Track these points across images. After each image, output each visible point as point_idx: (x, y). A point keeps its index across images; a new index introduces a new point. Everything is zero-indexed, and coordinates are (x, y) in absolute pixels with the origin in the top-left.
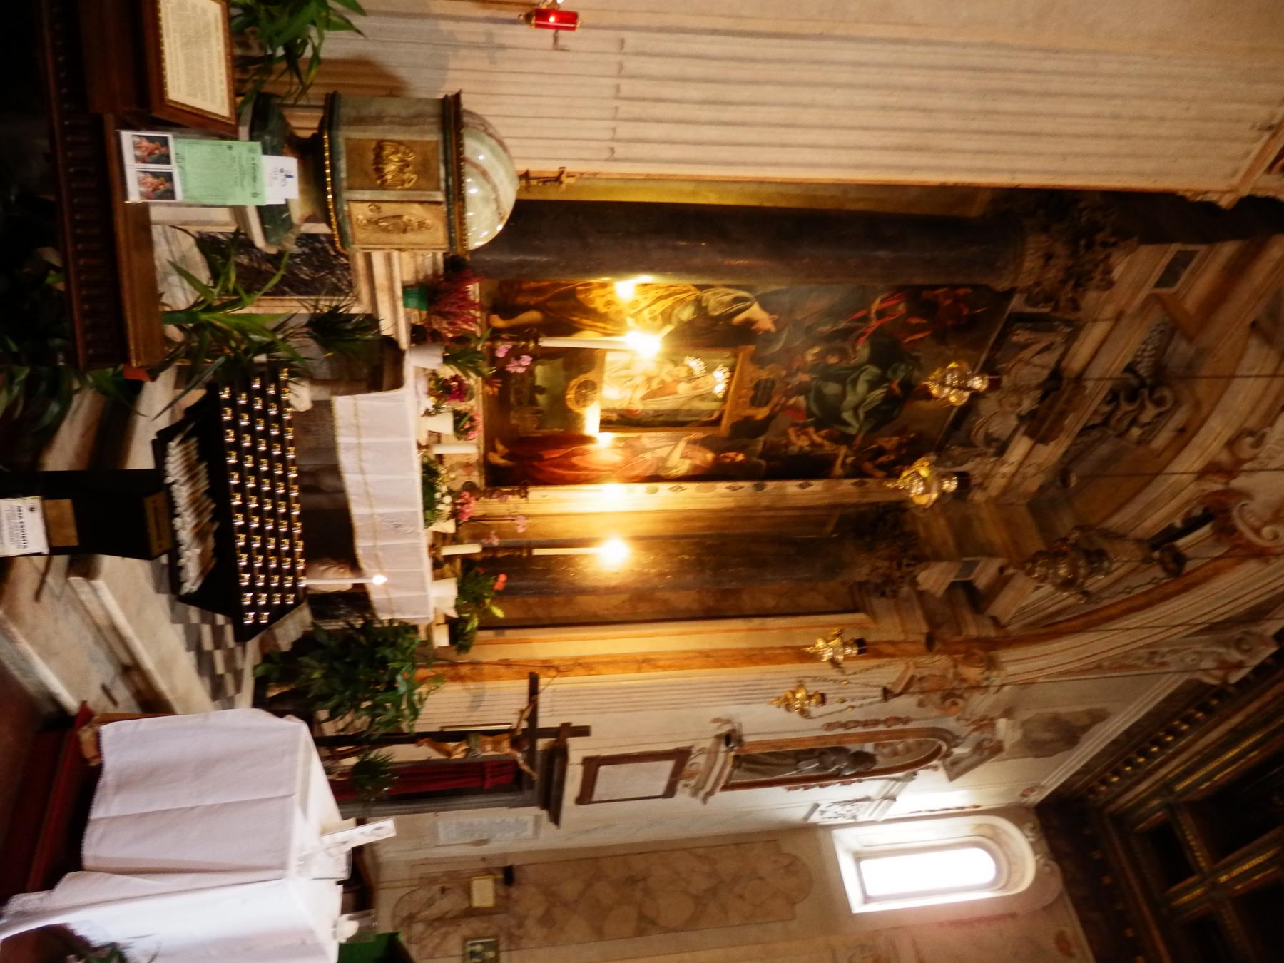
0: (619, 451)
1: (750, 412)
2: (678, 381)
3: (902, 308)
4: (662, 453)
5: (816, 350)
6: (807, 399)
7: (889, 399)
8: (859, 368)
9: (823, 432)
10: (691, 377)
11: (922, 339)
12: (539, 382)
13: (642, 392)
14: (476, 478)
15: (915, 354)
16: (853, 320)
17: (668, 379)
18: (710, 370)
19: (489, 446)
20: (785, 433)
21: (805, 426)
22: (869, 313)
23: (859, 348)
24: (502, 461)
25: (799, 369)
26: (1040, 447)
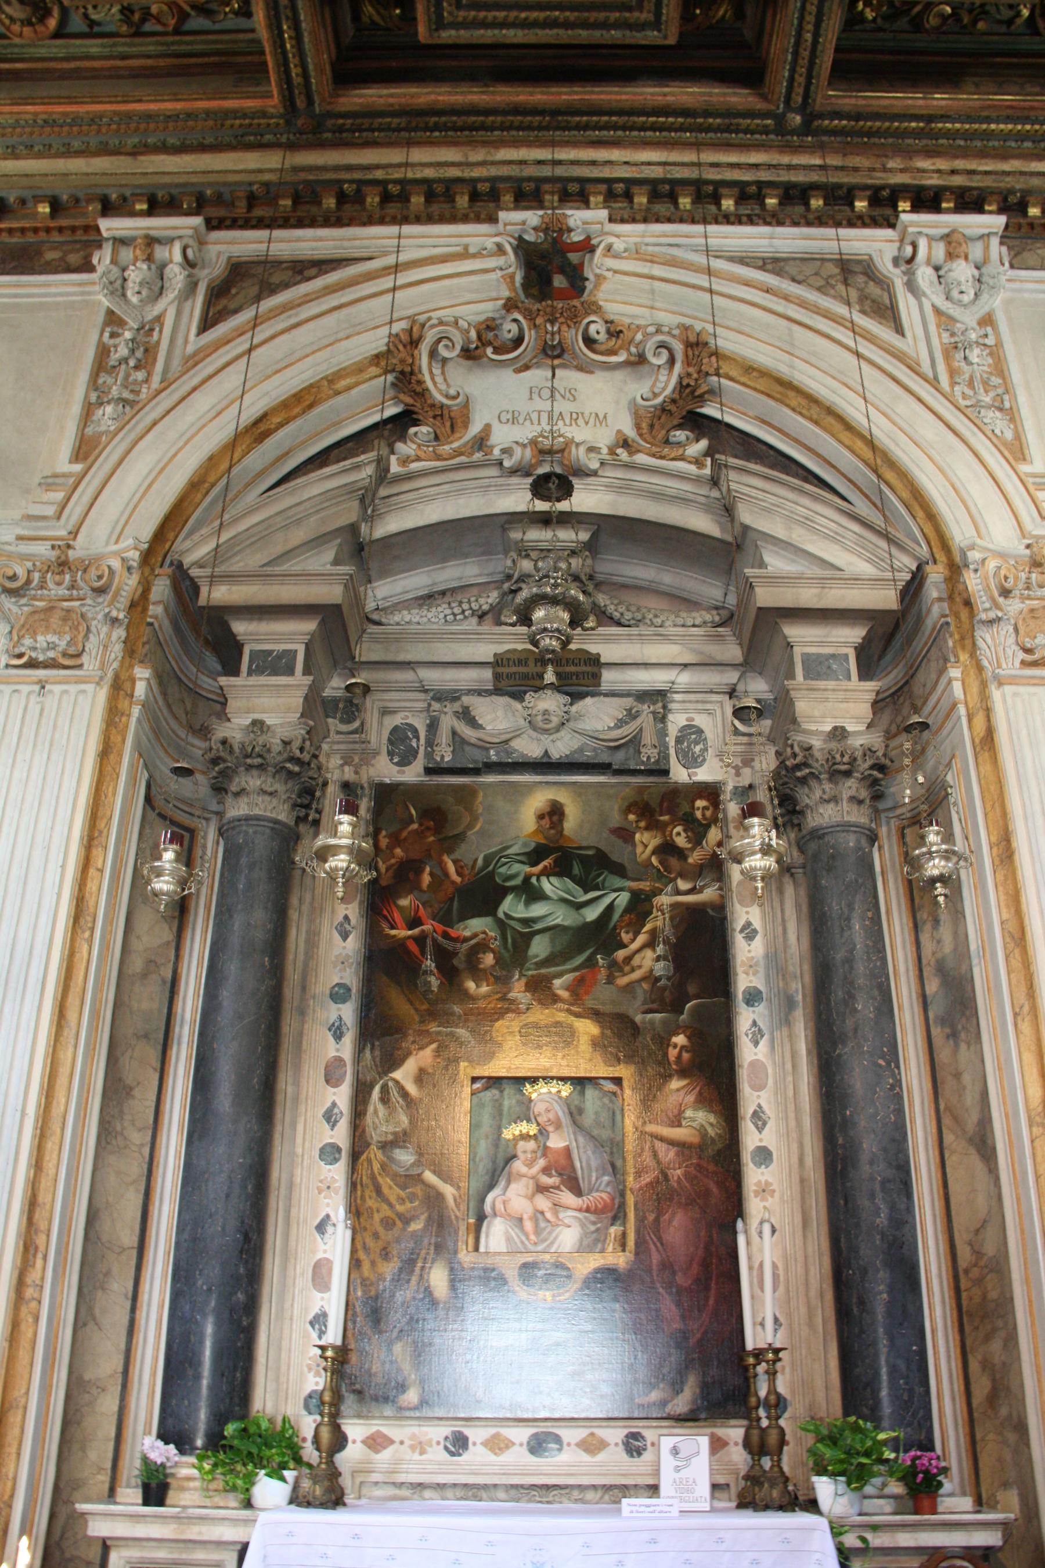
1: (584, 1044)
3: (404, 902)
4: (667, 1155)
5: (471, 985)
6: (560, 975)
7: (561, 870)
8: (502, 925)
9: (625, 937)
11: (455, 862)
13: (567, 1197)
15: (480, 862)
16: (423, 953)
17: (542, 1163)
20: (629, 988)
21: (613, 965)
22: (409, 937)
23: (467, 933)
25: (504, 998)
26: (603, 660)
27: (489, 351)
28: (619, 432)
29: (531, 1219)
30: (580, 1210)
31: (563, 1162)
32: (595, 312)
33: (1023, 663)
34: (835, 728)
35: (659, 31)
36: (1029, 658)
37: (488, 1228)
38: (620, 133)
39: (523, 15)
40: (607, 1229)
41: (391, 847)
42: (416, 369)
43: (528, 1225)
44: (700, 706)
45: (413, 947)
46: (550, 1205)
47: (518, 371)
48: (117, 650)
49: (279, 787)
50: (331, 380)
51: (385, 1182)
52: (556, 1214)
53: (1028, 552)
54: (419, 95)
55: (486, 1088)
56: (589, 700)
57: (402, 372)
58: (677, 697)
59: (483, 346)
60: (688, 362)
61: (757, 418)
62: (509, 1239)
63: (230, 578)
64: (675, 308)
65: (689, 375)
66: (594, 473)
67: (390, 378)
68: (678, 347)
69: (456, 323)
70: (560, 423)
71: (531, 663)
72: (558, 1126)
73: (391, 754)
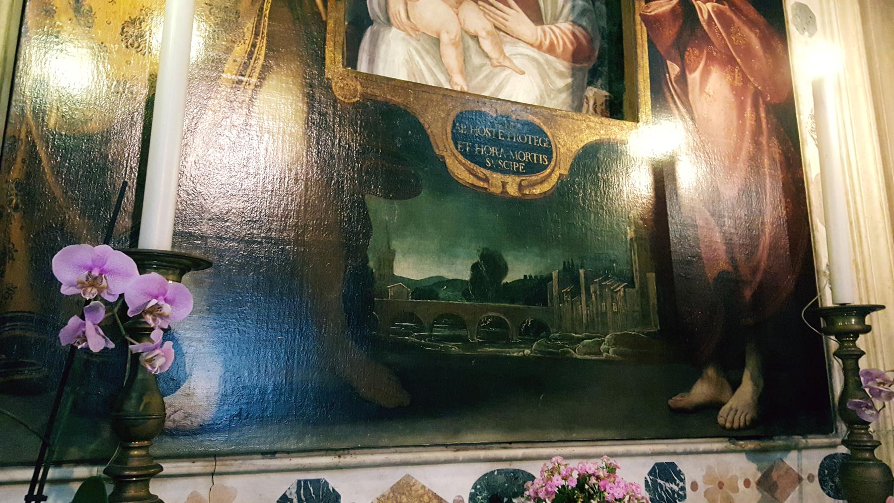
0: (694, 77)
12: (460, 270)
14: (807, 459)
19: (701, 422)
24: (747, 390)
29: (455, 44)
30: (540, 47)
37: (374, 45)
40: (583, 90)
43: (451, 56)
46: (490, 27)
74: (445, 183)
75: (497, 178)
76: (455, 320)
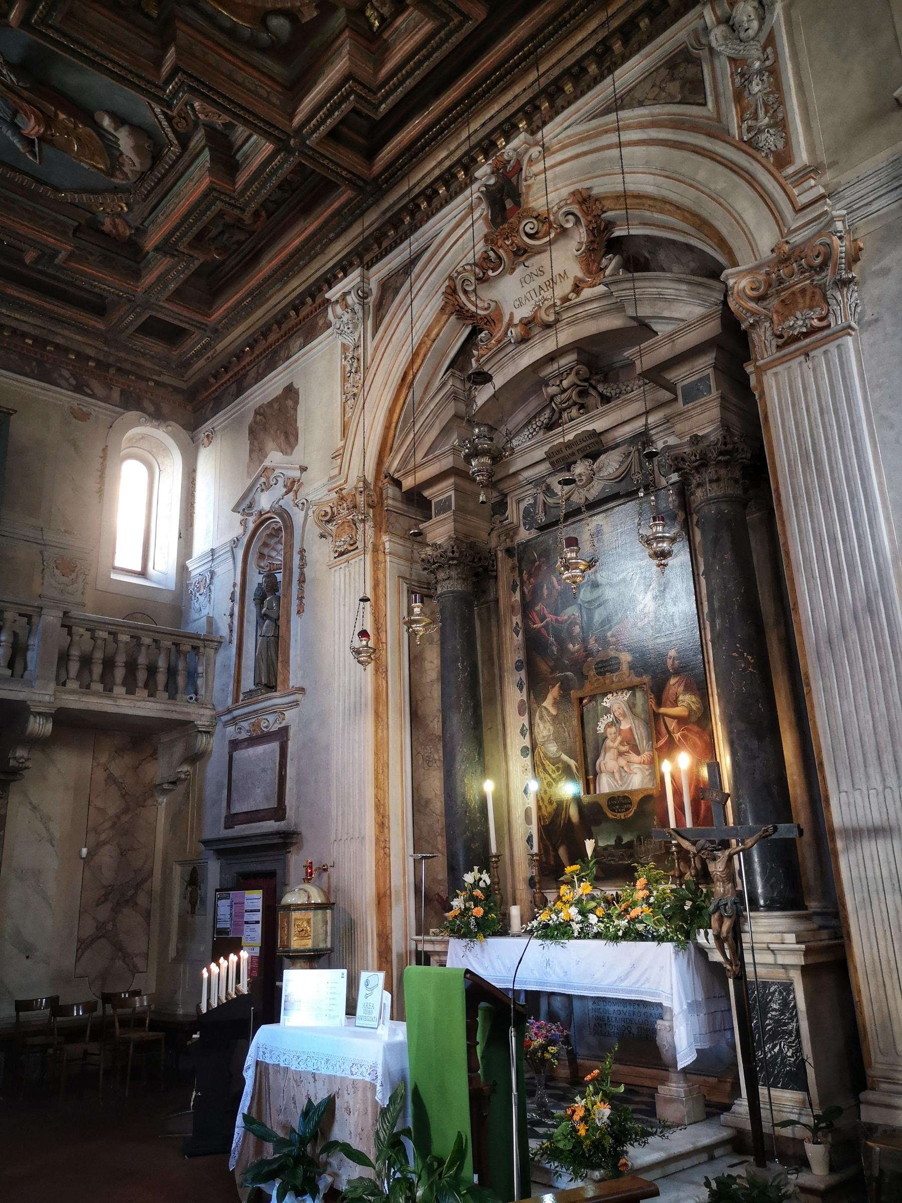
2: (620, 731)
10: (616, 722)
13: (634, 757)
17: (619, 739)
18: (607, 711)
23: (566, 617)
27: (490, 273)
28: (576, 277)
31: (629, 736)
32: (527, 217)
33: (779, 347)
34: (691, 437)
35: (471, 19)
36: (781, 341)
38: (508, 77)
39: (404, 72)
41: (529, 579)
42: (462, 306)
43: (617, 776)
44: (666, 432)
45: (544, 631)
47: (511, 273)
48: (370, 532)
49: (453, 573)
50: (427, 335)
51: (546, 762)
52: (629, 767)
53: (774, 255)
54: (404, 137)
55: (590, 701)
56: (603, 457)
57: (458, 311)
58: (652, 432)
59: (487, 269)
60: (586, 214)
61: (641, 224)
62: (609, 785)
63: (415, 469)
64: (568, 182)
65: (591, 222)
66: (557, 321)
67: (453, 317)
68: (575, 208)
69: (465, 269)
70: (542, 292)
71: (564, 450)
72: (624, 716)
73: (525, 524)
74: (608, 819)
75: (618, 814)
76: (611, 855)
